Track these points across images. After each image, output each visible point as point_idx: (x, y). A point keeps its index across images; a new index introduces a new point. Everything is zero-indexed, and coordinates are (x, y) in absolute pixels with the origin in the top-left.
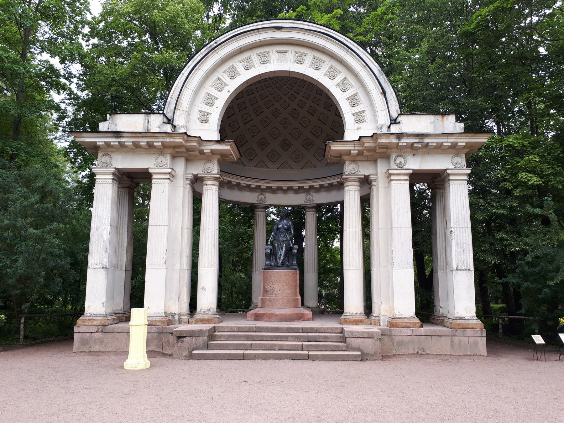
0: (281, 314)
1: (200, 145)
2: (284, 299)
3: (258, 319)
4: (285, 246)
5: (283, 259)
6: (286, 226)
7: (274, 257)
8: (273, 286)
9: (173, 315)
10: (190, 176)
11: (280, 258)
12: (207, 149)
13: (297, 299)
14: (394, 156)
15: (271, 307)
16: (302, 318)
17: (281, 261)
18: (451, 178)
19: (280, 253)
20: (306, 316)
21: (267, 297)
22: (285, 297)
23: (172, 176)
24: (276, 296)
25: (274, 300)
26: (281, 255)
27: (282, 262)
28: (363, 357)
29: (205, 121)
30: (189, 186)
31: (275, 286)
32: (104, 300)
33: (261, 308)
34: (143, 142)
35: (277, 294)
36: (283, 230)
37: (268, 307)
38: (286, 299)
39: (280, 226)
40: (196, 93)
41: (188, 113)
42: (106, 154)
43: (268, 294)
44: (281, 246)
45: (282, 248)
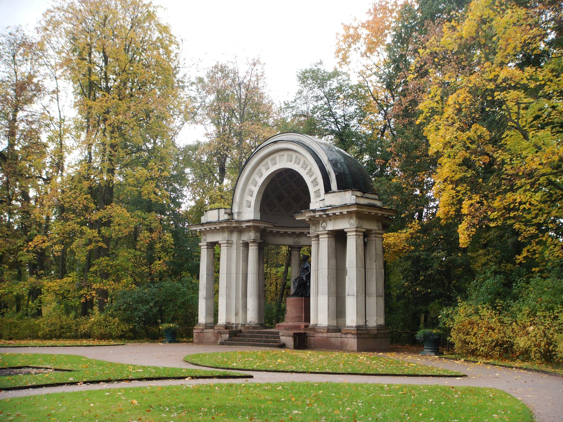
1: (240, 224)
9: (233, 324)
10: (241, 242)
12: (244, 225)
13: (302, 317)
14: (321, 222)
18: (348, 234)
23: (229, 243)
28: (283, 346)
29: (250, 206)
30: (242, 248)
32: (205, 315)
34: (213, 227)
40: (244, 190)
41: (241, 204)
42: (204, 235)
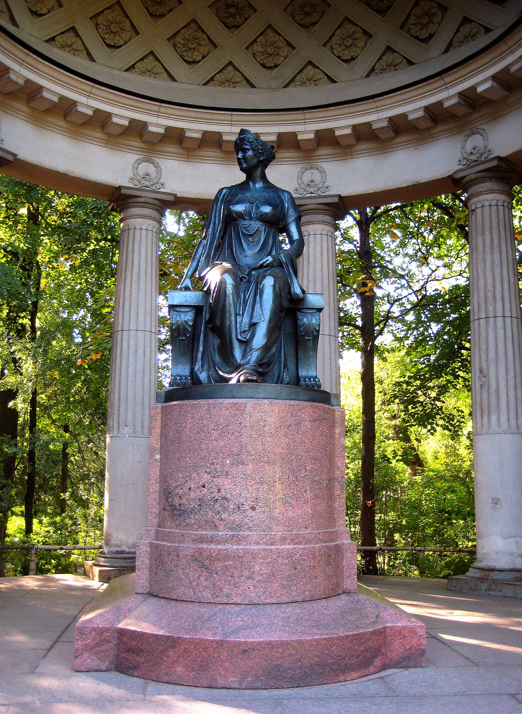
0: (271, 645)
2: (279, 554)
3: (136, 667)
4: (274, 286)
5: (266, 348)
6: (267, 209)
7: (215, 341)
8: (219, 481)
11: (246, 344)
15: (207, 595)
16: (376, 652)
17: (254, 356)
19: (246, 320)
20: (396, 644)
21: (183, 538)
22: (283, 540)
24: (238, 540)
25: (227, 556)
26: (253, 326)
27: (260, 363)
31: (226, 484)
33: (151, 594)
35: (240, 526)
36: (256, 225)
37: (189, 594)
38: (290, 555)
39: (239, 208)
43: (190, 526)
44: (252, 287)
45: (259, 292)
